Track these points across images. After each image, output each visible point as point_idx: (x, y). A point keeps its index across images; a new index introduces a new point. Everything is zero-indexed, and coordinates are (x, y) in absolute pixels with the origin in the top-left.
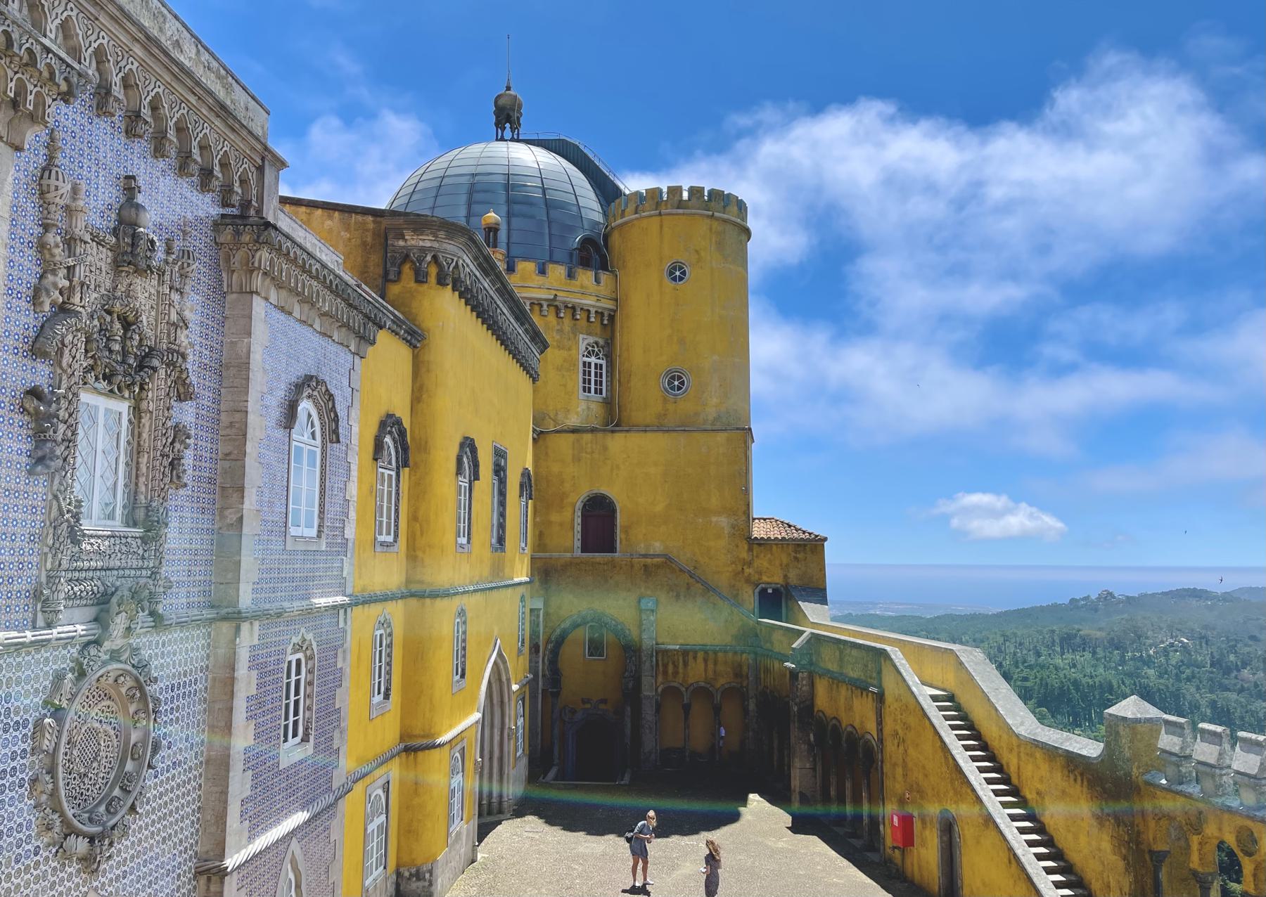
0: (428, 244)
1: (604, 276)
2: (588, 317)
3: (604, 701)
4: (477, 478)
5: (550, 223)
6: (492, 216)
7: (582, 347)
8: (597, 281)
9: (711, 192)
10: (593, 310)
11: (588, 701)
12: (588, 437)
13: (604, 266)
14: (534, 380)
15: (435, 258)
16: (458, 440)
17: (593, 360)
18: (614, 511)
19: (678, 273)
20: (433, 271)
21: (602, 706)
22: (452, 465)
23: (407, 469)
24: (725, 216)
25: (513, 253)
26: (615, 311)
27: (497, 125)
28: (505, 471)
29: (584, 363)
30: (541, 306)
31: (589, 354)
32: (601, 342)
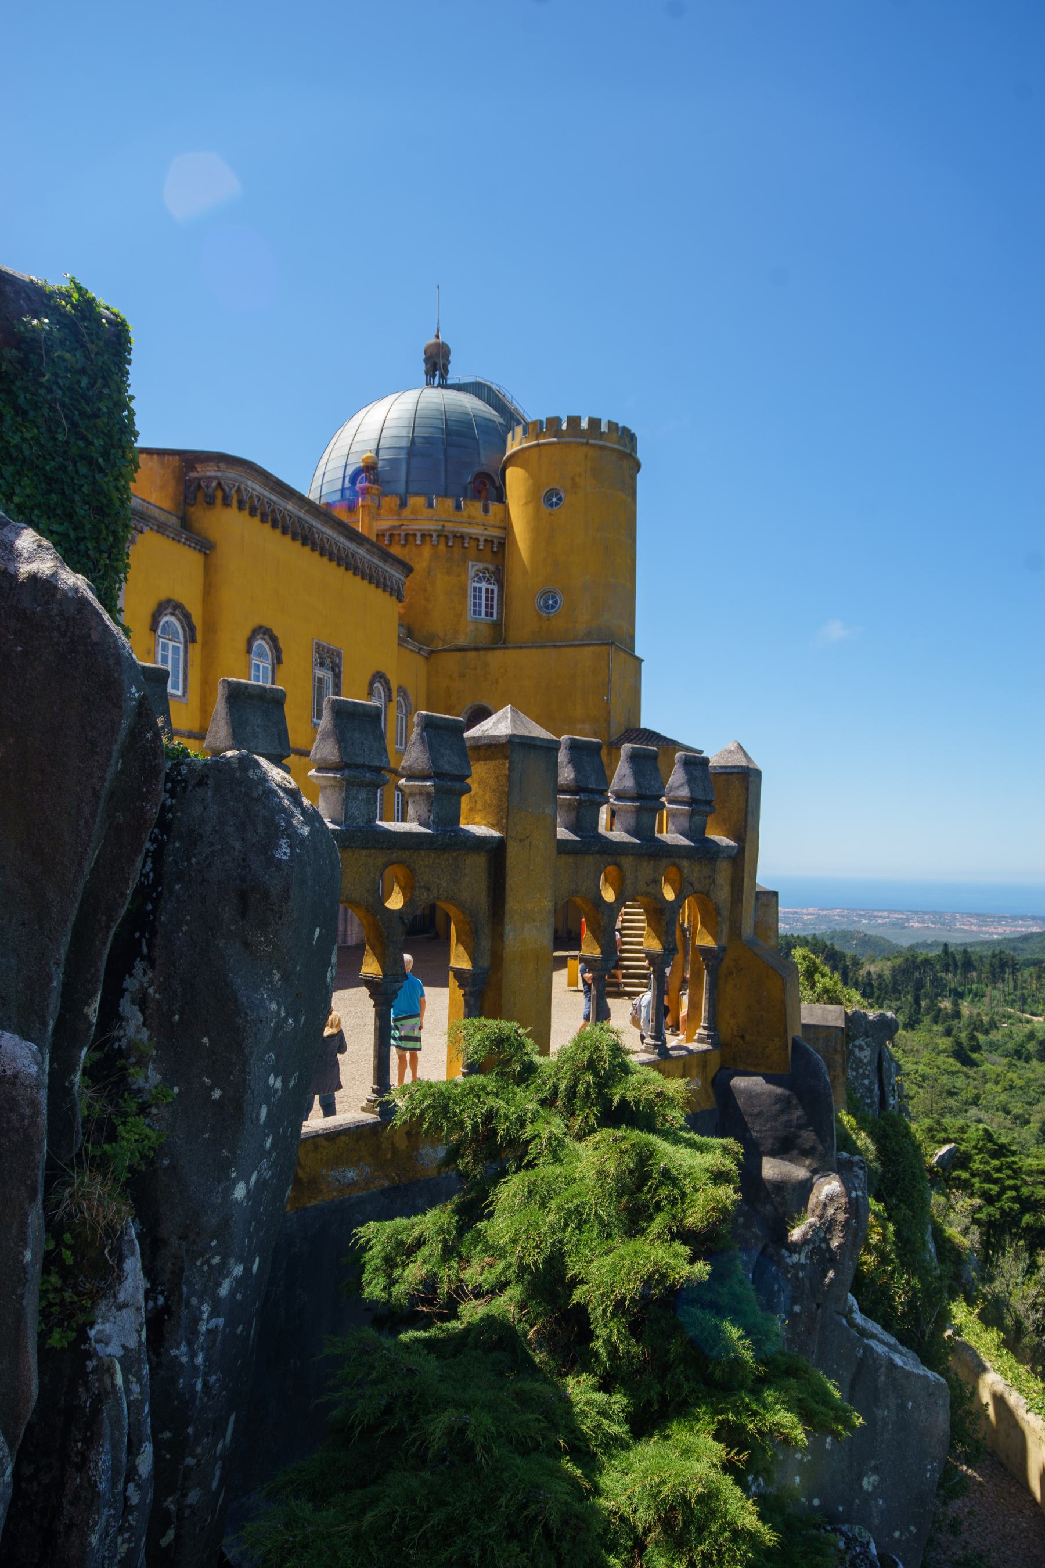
0: (213, 474)
7: (472, 572)
8: (486, 510)
10: (482, 539)
12: (471, 654)
15: (219, 484)
17: (484, 585)
19: (554, 499)
20: (219, 494)
22: (242, 645)
23: (198, 647)
24: (601, 443)
27: (427, 373)
29: (475, 588)
30: (431, 536)
31: (480, 581)
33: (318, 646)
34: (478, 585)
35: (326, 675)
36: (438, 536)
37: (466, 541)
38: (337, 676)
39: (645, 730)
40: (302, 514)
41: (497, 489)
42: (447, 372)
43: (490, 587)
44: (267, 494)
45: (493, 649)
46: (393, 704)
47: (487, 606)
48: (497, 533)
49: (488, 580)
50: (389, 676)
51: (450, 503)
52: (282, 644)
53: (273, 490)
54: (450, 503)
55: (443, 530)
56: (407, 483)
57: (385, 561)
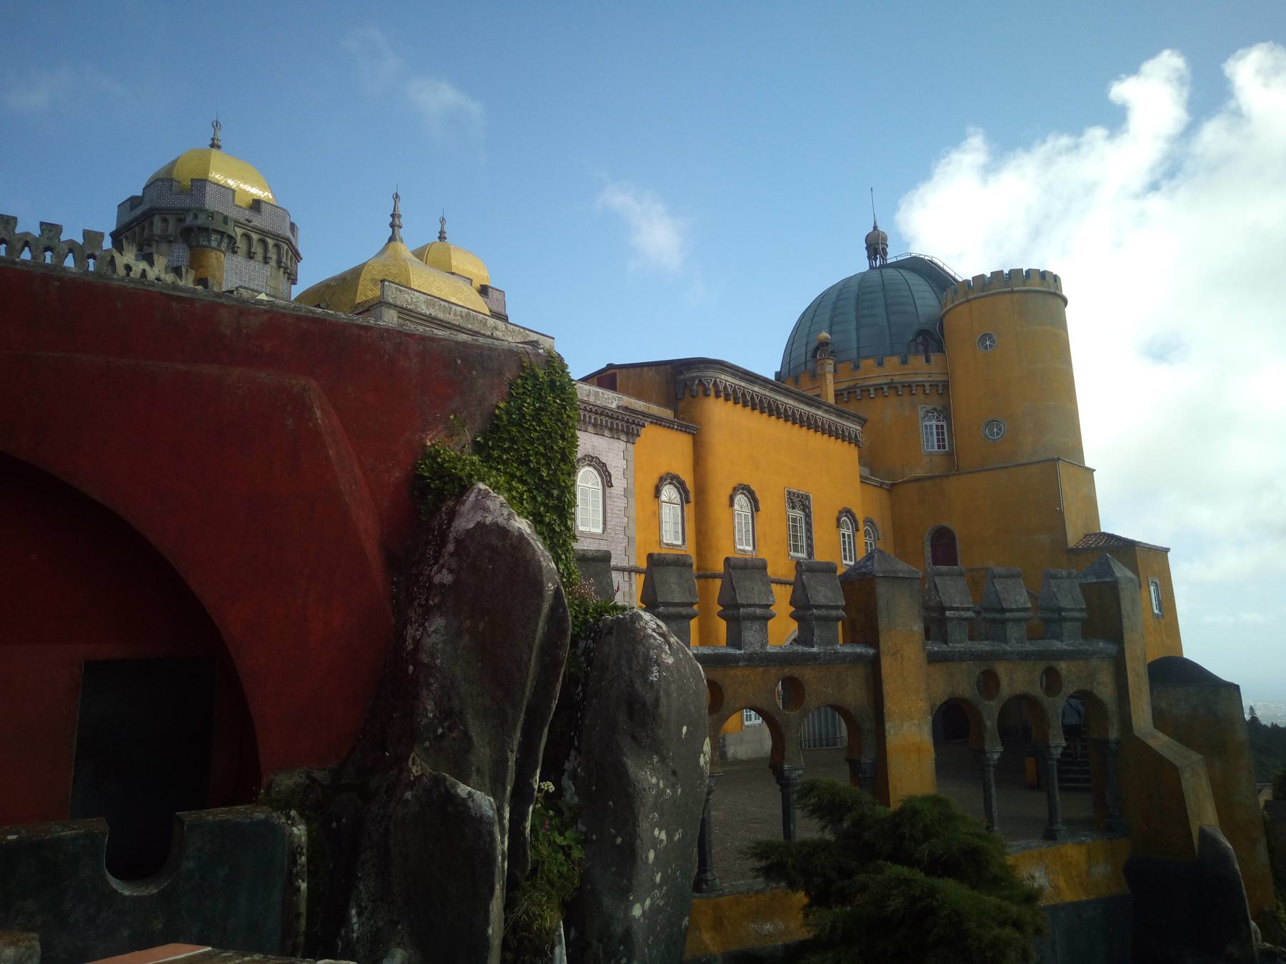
4: (757, 510)
7: (921, 413)
8: (928, 361)
9: (1011, 271)
10: (927, 385)
13: (941, 349)
15: (700, 381)
16: (734, 483)
17: (934, 423)
18: (954, 539)
20: (701, 389)
22: (726, 500)
32: (939, 408)
33: (789, 493)
35: (798, 513)
38: (808, 516)
39: (1105, 534)
44: (737, 382)
45: (947, 476)
46: (861, 532)
48: (942, 378)
50: (854, 510)
51: (895, 360)
52: (758, 495)
53: (742, 379)
54: (895, 360)
55: (892, 382)
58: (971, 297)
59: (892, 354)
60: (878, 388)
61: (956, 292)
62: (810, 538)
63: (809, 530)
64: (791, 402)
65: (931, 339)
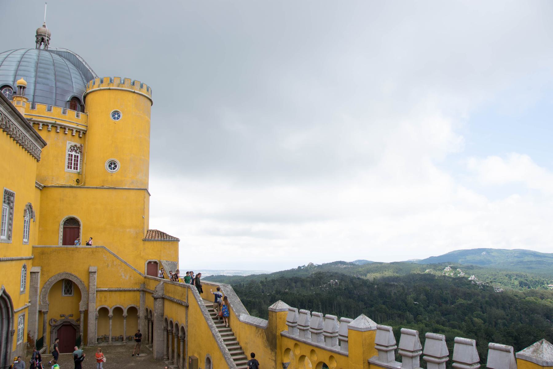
1: (81, 114)
2: (72, 133)
3: (71, 316)
5: (56, 88)
6: (22, 81)
7: (68, 147)
8: (77, 116)
11: (63, 316)
13: (83, 111)
14: (38, 161)
17: (74, 153)
18: (79, 225)
19: (116, 116)
21: (70, 318)
25: (36, 100)
26: (86, 131)
27: (37, 42)
28: (12, 202)
29: (69, 154)
32: (78, 145)
33: (5, 190)
34: (71, 153)
35: (6, 206)
36: (52, 126)
37: (67, 130)
38: (12, 208)
40: (6, 114)
41: (81, 106)
42: (49, 44)
43: (77, 154)
47: (74, 164)
49: (76, 151)
50: (33, 205)
54: (61, 110)
55: (55, 124)
56: (34, 96)
57: (36, 140)
58: (111, 88)
59: (56, 105)
60: (45, 125)
61: (102, 82)
62: (10, 225)
63: (11, 219)
64: (16, 124)
65: (77, 103)
